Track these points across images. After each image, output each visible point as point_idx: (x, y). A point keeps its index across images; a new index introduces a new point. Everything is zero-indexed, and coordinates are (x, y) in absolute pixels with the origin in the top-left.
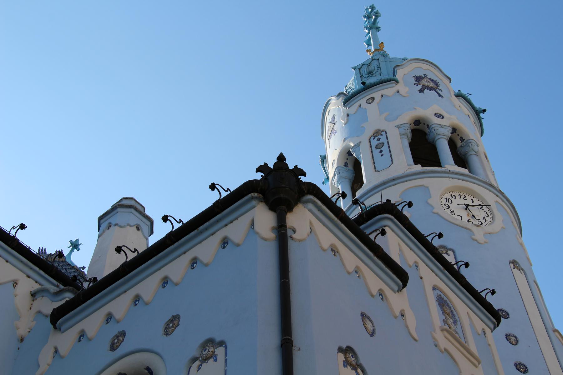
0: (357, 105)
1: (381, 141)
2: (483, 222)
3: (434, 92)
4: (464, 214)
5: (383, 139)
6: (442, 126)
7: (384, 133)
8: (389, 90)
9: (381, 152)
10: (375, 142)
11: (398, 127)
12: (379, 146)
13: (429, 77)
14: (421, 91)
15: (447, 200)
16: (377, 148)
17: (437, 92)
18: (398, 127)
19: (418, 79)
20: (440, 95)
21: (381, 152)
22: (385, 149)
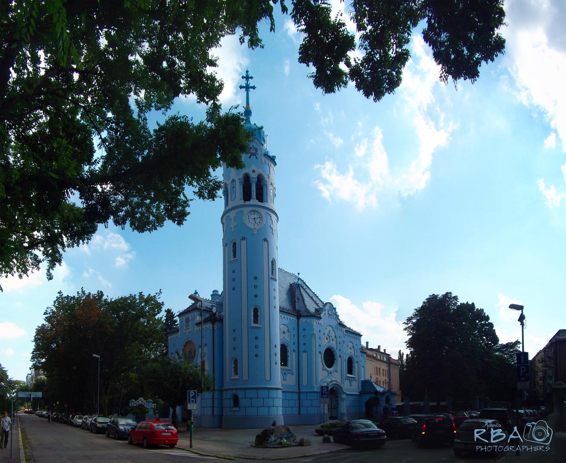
10: (232, 185)
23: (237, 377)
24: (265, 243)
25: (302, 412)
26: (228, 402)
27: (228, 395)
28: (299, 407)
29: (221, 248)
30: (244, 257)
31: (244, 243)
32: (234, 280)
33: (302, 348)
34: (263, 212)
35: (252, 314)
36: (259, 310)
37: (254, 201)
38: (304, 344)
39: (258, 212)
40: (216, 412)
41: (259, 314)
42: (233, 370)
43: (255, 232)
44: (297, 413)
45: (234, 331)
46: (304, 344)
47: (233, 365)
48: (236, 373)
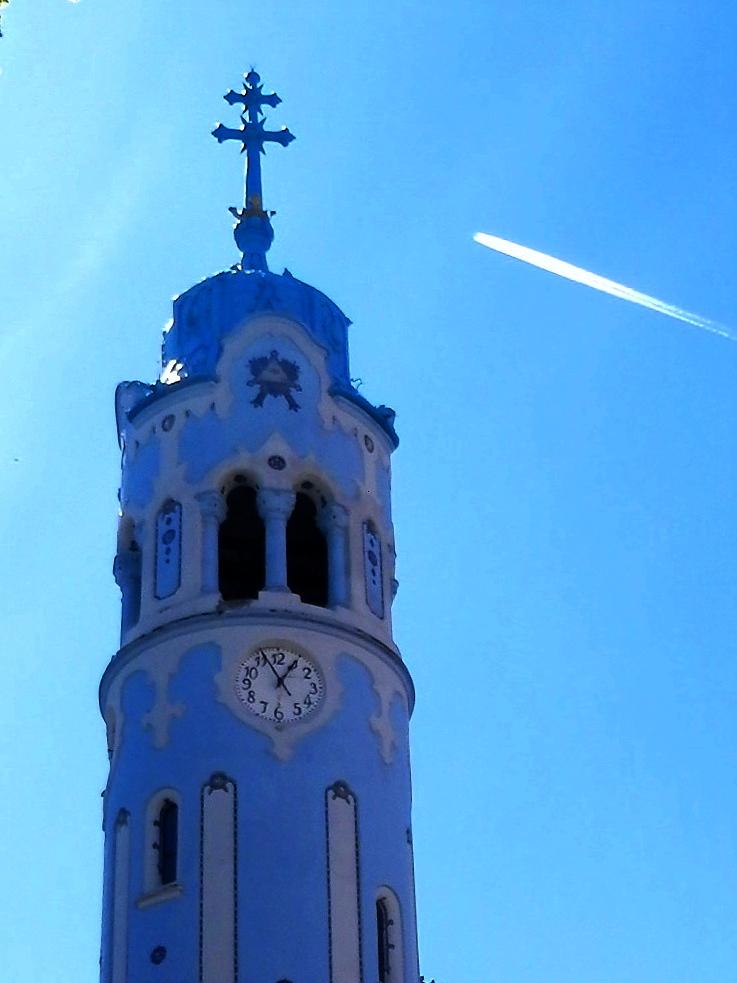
0: (147, 426)
1: (171, 527)
5: (174, 525)
6: (277, 492)
7: (177, 508)
9: (168, 551)
10: (163, 528)
11: (199, 497)
12: (170, 535)
13: (280, 358)
14: (258, 401)
15: (249, 672)
16: (165, 542)
18: (199, 497)
19: (257, 365)
20: (293, 406)
21: (168, 551)
22: (173, 545)
24: (340, 808)
29: (98, 837)
31: (218, 804)
34: (326, 648)
37: (277, 597)
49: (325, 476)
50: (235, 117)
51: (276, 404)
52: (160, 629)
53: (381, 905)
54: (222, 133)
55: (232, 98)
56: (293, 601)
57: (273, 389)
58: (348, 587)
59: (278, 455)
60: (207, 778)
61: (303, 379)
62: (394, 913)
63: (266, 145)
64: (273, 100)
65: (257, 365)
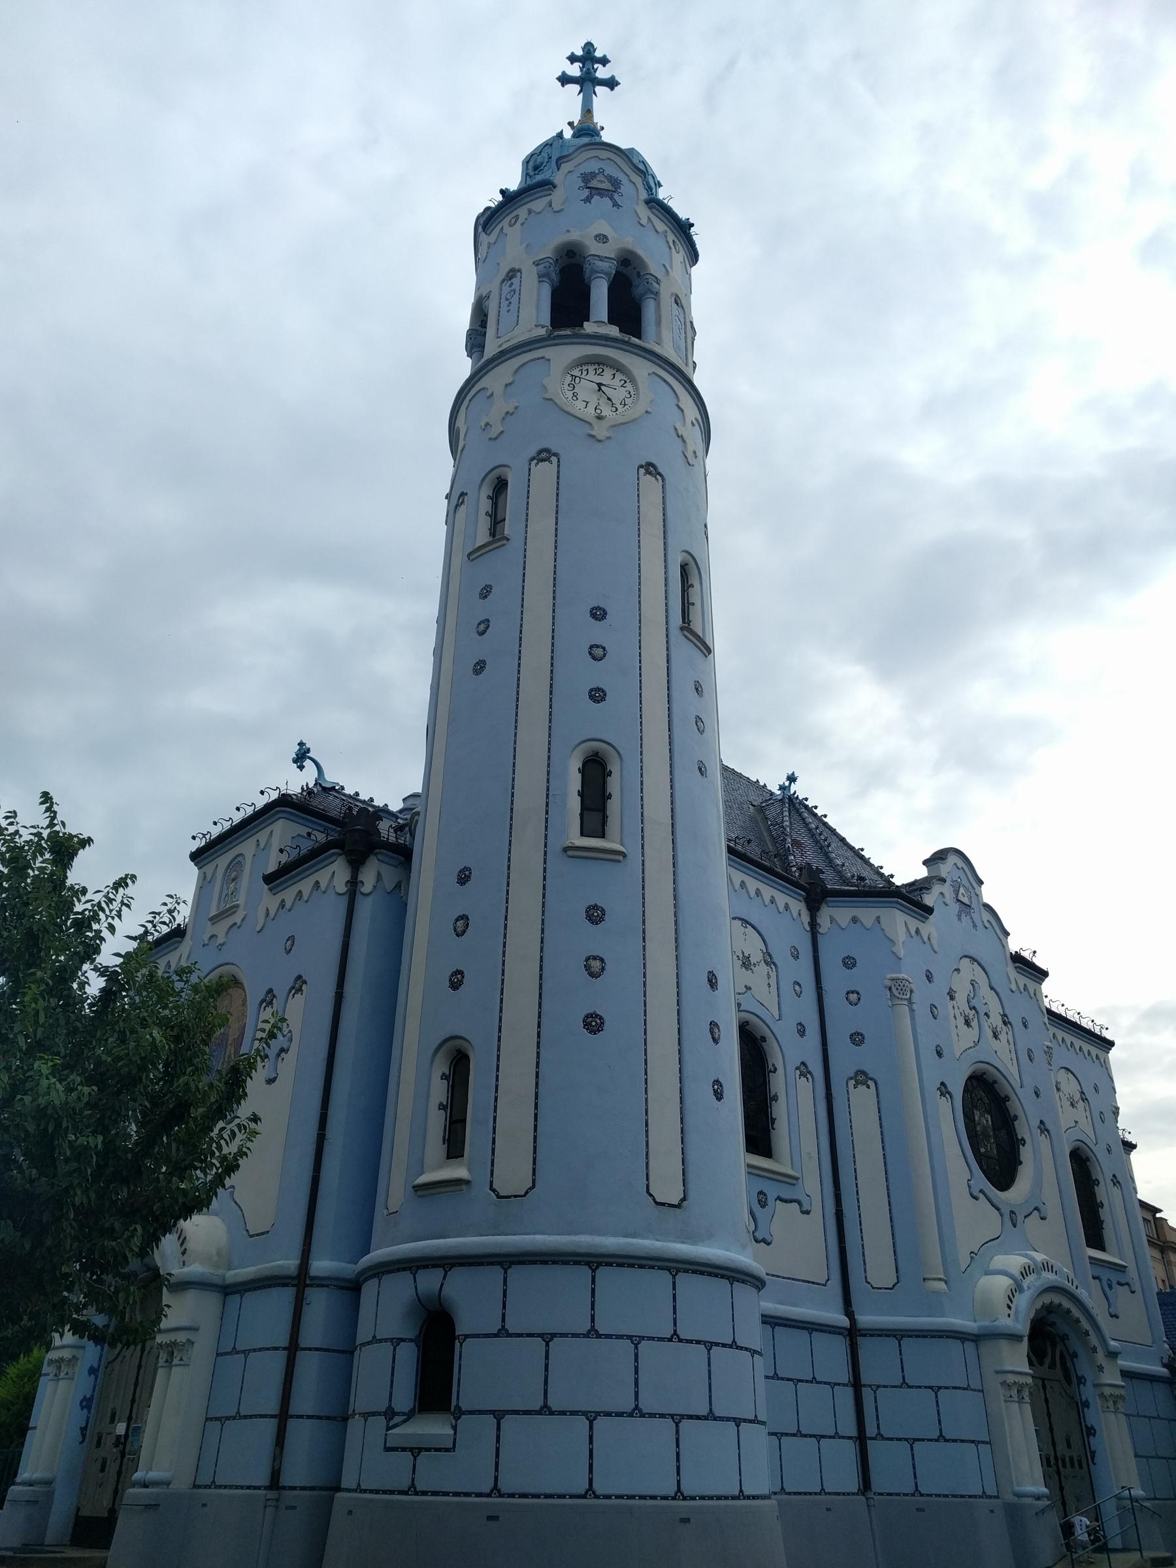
2: (620, 407)
3: (607, 200)
4: (593, 399)
6: (601, 259)
8: (538, 205)
11: (537, 264)
14: (588, 200)
15: (574, 377)
17: (612, 198)
18: (537, 264)
19: (587, 178)
20: (616, 205)
22: (514, 300)
23: (458, 1171)
25: (879, 1483)
26: (385, 1372)
27: (388, 1310)
28: (862, 1439)
30: (541, 526)
32: (484, 627)
33: (845, 1060)
34: (641, 368)
35: (575, 782)
36: (614, 766)
38: (857, 1039)
39: (619, 368)
40: (300, 1469)
41: (613, 785)
42: (436, 1122)
43: (600, 431)
44: (852, 1483)
45: (464, 877)
46: (857, 1039)
47: (439, 1091)
48: (454, 1147)
49: (640, 252)
50: (575, 70)
51: (602, 204)
52: (502, 353)
53: (684, 568)
54: (564, 80)
55: (573, 59)
56: (614, 331)
57: (600, 192)
58: (659, 333)
59: (605, 232)
60: (532, 452)
61: (622, 189)
62: (694, 580)
63: (598, 89)
64: (604, 61)
65: (587, 178)
